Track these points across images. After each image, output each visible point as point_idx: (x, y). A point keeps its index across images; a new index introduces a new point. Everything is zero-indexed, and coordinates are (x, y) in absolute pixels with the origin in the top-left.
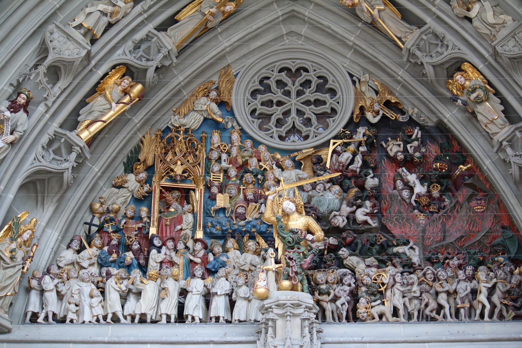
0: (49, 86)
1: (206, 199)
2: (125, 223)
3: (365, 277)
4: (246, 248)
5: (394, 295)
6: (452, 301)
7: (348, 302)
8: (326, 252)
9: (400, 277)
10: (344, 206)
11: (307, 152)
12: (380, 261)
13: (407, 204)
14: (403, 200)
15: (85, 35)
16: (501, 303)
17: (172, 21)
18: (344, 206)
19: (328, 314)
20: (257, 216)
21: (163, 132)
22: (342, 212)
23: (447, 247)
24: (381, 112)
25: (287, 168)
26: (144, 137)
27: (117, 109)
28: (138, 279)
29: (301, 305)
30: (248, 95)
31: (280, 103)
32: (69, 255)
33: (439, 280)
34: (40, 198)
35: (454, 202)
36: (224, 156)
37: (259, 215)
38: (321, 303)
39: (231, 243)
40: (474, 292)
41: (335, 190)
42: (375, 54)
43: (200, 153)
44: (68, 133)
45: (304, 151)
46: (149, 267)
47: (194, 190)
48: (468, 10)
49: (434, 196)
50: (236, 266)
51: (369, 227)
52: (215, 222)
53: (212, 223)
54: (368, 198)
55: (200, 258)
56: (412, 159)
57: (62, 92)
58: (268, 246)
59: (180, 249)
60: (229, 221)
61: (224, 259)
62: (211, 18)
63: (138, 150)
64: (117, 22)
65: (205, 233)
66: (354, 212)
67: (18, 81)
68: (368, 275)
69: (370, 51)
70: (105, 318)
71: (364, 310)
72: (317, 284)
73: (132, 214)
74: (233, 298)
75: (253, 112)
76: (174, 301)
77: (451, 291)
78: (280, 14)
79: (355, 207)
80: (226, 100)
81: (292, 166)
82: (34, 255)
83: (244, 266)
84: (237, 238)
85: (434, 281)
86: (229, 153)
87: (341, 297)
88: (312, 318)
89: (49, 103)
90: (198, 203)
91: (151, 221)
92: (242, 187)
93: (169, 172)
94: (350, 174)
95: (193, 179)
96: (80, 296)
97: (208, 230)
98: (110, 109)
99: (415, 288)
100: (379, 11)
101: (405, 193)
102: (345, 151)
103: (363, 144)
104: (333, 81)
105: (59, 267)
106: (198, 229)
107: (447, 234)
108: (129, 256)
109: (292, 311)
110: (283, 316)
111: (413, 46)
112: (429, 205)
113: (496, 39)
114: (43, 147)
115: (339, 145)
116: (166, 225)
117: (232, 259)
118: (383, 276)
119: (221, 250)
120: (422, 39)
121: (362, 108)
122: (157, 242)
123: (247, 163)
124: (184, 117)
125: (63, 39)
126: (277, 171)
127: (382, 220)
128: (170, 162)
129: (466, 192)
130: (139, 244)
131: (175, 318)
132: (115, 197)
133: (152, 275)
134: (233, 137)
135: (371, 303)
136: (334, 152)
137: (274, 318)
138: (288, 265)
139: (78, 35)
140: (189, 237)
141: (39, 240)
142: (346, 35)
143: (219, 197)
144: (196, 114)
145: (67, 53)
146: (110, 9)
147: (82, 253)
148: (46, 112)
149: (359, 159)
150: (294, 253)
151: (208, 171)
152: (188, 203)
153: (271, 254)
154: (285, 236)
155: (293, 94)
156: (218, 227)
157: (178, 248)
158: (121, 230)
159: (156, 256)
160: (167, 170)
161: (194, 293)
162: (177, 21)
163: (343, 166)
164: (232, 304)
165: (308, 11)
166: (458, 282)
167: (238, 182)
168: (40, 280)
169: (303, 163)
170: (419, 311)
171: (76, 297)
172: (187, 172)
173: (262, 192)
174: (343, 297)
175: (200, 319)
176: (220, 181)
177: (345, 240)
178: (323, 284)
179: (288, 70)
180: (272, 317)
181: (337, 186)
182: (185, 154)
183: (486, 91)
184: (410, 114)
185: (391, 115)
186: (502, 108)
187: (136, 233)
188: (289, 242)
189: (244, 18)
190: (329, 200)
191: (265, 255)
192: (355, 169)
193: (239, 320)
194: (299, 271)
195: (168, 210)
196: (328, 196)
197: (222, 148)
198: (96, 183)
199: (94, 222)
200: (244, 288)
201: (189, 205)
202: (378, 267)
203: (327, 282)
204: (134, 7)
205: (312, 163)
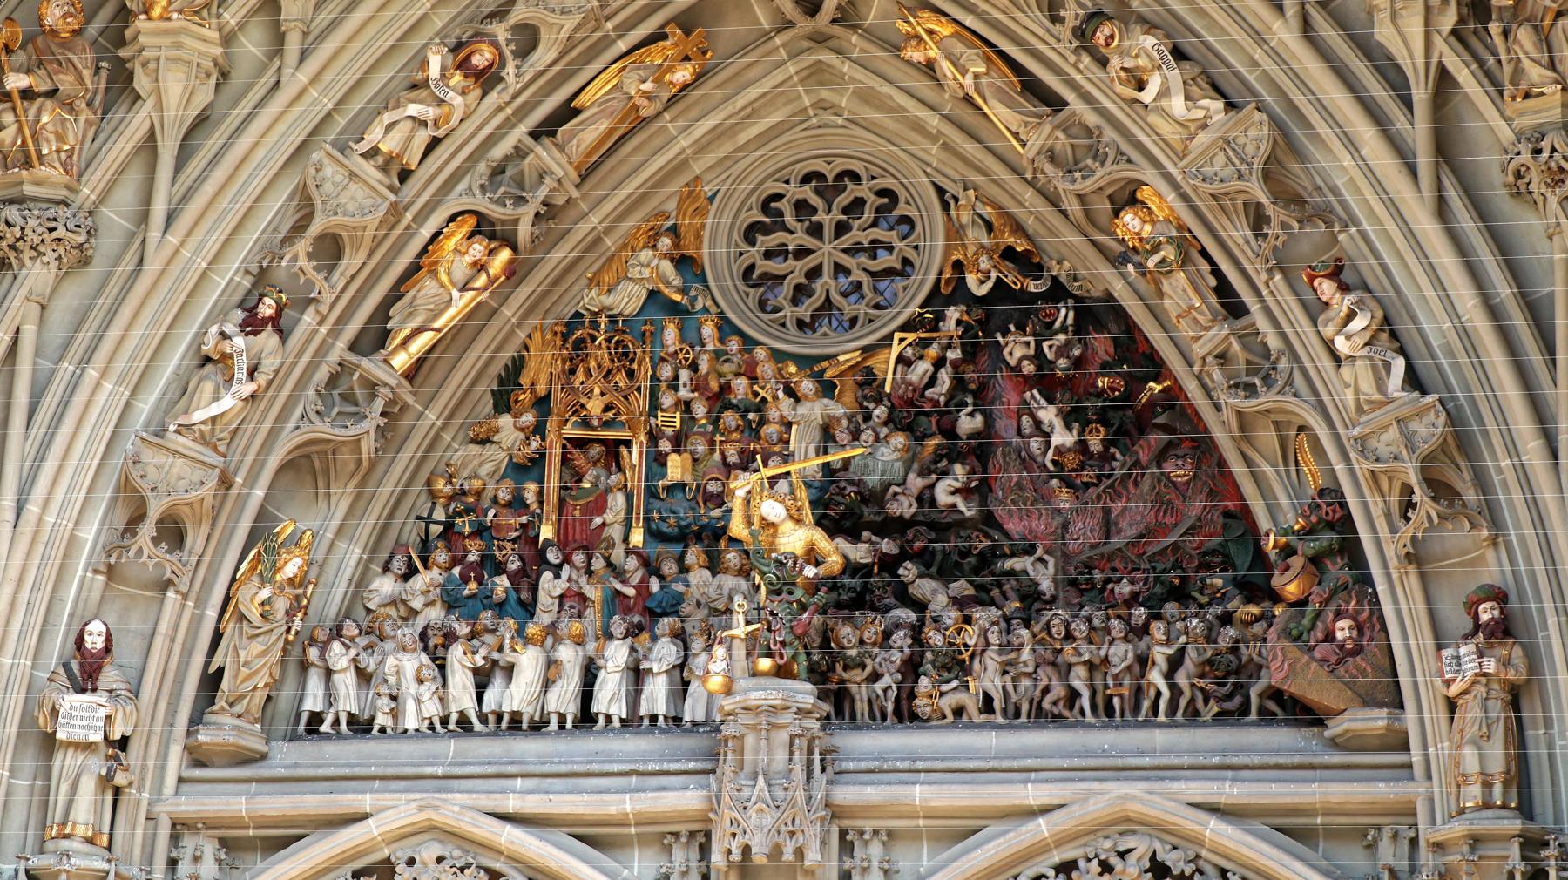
2: (495, 516)
8: (876, 568)
10: (911, 476)
11: (847, 361)
12: (979, 587)
15: (384, 169)
16: (1193, 685)
17: (567, 112)
19: (861, 707)
21: (568, 324)
24: (994, 275)
26: (530, 336)
29: (789, 708)
30: (735, 236)
31: (802, 253)
32: (385, 586)
36: (684, 375)
40: (1144, 661)
43: (639, 366)
44: (365, 363)
45: (841, 358)
46: (539, 606)
47: (628, 444)
48: (1141, 87)
49: (1092, 449)
50: (703, 601)
53: (659, 512)
57: (348, 283)
61: (680, 587)
63: (518, 365)
66: (932, 487)
67: (261, 267)
70: (445, 721)
73: (508, 497)
75: (751, 268)
76: (571, 687)
77: (1097, 661)
80: (690, 252)
82: (309, 602)
86: (694, 367)
89: (324, 309)
96: (399, 680)
97: (654, 526)
99: (1026, 655)
100: (976, 76)
101: (1035, 444)
102: (921, 357)
104: (908, 203)
105: (369, 611)
107: (1113, 528)
108: (503, 582)
110: (754, 728)
111: (1039, 153)
115: (910, 345)
119: (675, 568)
121: (958, 266)
122: (553, 556)
124: (609, 291)
126: (785, 403)
129: (1156, 438)
130: (521, 558)
131: (575, 717)
134: (703, 331)
136: (901, 359)
138: (769, 630)
139: (369, 170)
141: (321, 567)
146: (430, 113)
148: (320, 323)
149: (945, 376)
151: (655, 407)
155: (828, 232)
156: (672, 521)
163: (914, 390)
166: (1111, 643)
167: (710, 428)
168: (324, 647)
171: (392, 680)
175: (622, 720)
178: (851, 648)
179: (818, 176)
182: (609, 372)
184: (1054, 273)
185: (1012, 278)
186: (1213, 282)
187: (515, 534)
194: (789, 638)
197: (681, 356)
198: (437, 437)
203: (862, 642)
204: (483, 97)
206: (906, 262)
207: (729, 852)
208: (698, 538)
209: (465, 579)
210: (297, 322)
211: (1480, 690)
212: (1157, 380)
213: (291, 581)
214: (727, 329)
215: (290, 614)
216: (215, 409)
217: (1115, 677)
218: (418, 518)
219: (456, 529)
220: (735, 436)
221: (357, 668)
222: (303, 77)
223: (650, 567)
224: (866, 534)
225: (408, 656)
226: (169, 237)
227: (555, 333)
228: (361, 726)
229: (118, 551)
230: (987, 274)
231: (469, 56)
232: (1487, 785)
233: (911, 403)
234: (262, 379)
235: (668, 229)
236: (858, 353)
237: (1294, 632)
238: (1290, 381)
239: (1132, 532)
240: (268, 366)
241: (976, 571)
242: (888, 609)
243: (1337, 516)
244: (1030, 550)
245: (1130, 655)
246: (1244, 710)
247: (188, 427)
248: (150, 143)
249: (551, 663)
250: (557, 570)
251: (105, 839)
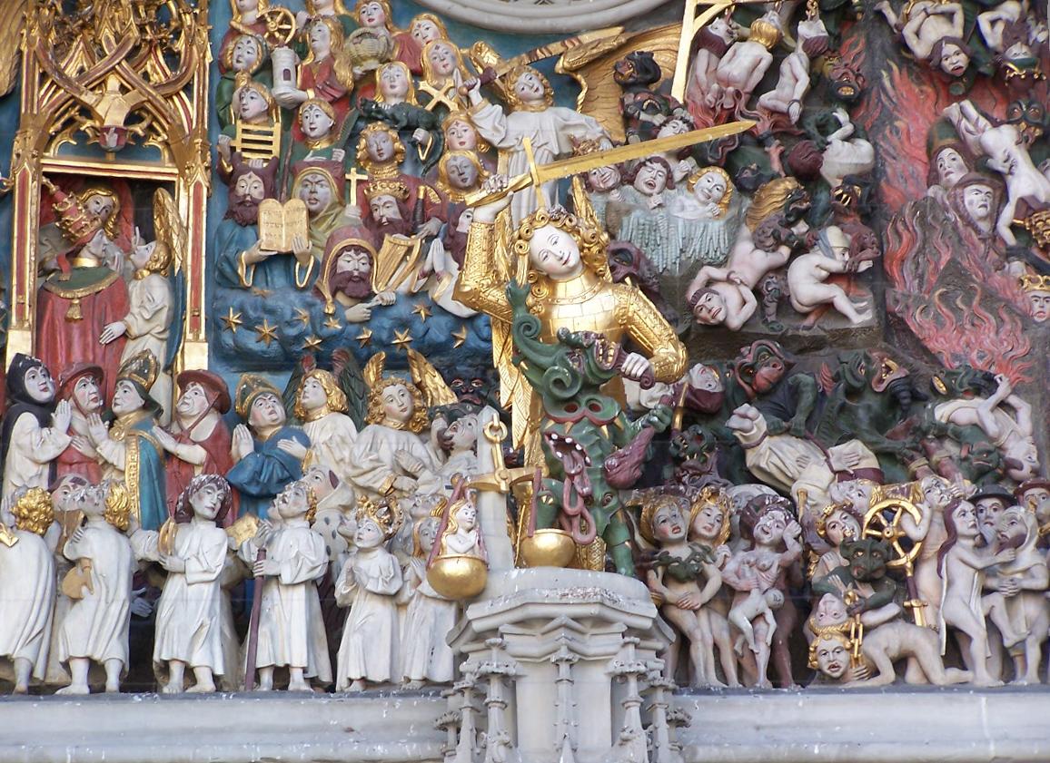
1: (217, 221)
3: (837, 516)
4: (377, 404)
5: (950, 584)
7: (777, 612)
8: (678, 419)
9: (970, 516)
11: (600, 41)
13: (984, 240)
14: (969, 223)
18: (745, 247)
19: (701, 655)
20: (410, 283)
22: (735, 268)
25: (524, 101)
36: (284, 58)
37: (423, 281)
38: (674, 613)
39: (319, 388)
41: (710, 186)
45: (586, 38)
50: (340, 475)
51: (841, 325)
52: (255, 309)
53: (241, 309)
54: (836, 215)
55: (202, 444)
56: (1000, 70)
58: (455, 400)
59: (123, 413)
60: (309, 306)
61: (293, 447)
65: (219, 352)
66: (782, 269)
68: (849, 510)
71: (838, 641)
72: (658, 544)
74: (337, 595)
79: (785, 251)
81: (544, 97)
83: (369, 476)
84: (339, 368)
86: (301, 48)
87: (748, 592)
88: (651, 670)
90: (186, 238)
91: (9, 306)
95: (166, 143)
97: (228, 339)
101: (976, 199)
102: (743, 39)
106: (189, 336)
110: (540, 661)
115: (720, 14)
116: (69, 320)
117: (324, 447)
118: (904, 511)
122: (36, 386)
123: (374, 85)
126: (488, 117)
127: (890, 302)
128: (80, 79)
133: (31, 511)
135: (862, 613)
136: (702, 40)
137: (512, 671)
138: (557, 473)
140: (157, 364)
143: (270, 212)
149: (796, 65)
150: (578, 426)
152: (148, 236)
153: (491, 427)
154: (543, 360)
156: (266, 329)
157: (116, 409)
159: (35, 438)
160: (66, 111)
161: (191, 578)
163: (738, 94)
164: (333, 617)
167: (340, 155)
169: (583, 82)
172: (141, 119)
173: (432, 194)
174: (755, 592)
175: (216, 678)
176: (270, 152)
177: (753, 376)
178: (678, 542)
180: (502, 670)
181: (718, 170)
182: (136, 49)
188: (559, 383)
190: (690, 223)
191: (448, 434)
192: (783, 107)
193: (363, 679)
195: (72, 263)
196: (683, 208)
197: (272, 25)
201: (153, 244)
202: (879, 477)
203: (692, 535)
205: (618, 82)
208: (324, 363)
241: (880, 424)
244: (983, 385)
249: (64, 566)
250: (45, 412)
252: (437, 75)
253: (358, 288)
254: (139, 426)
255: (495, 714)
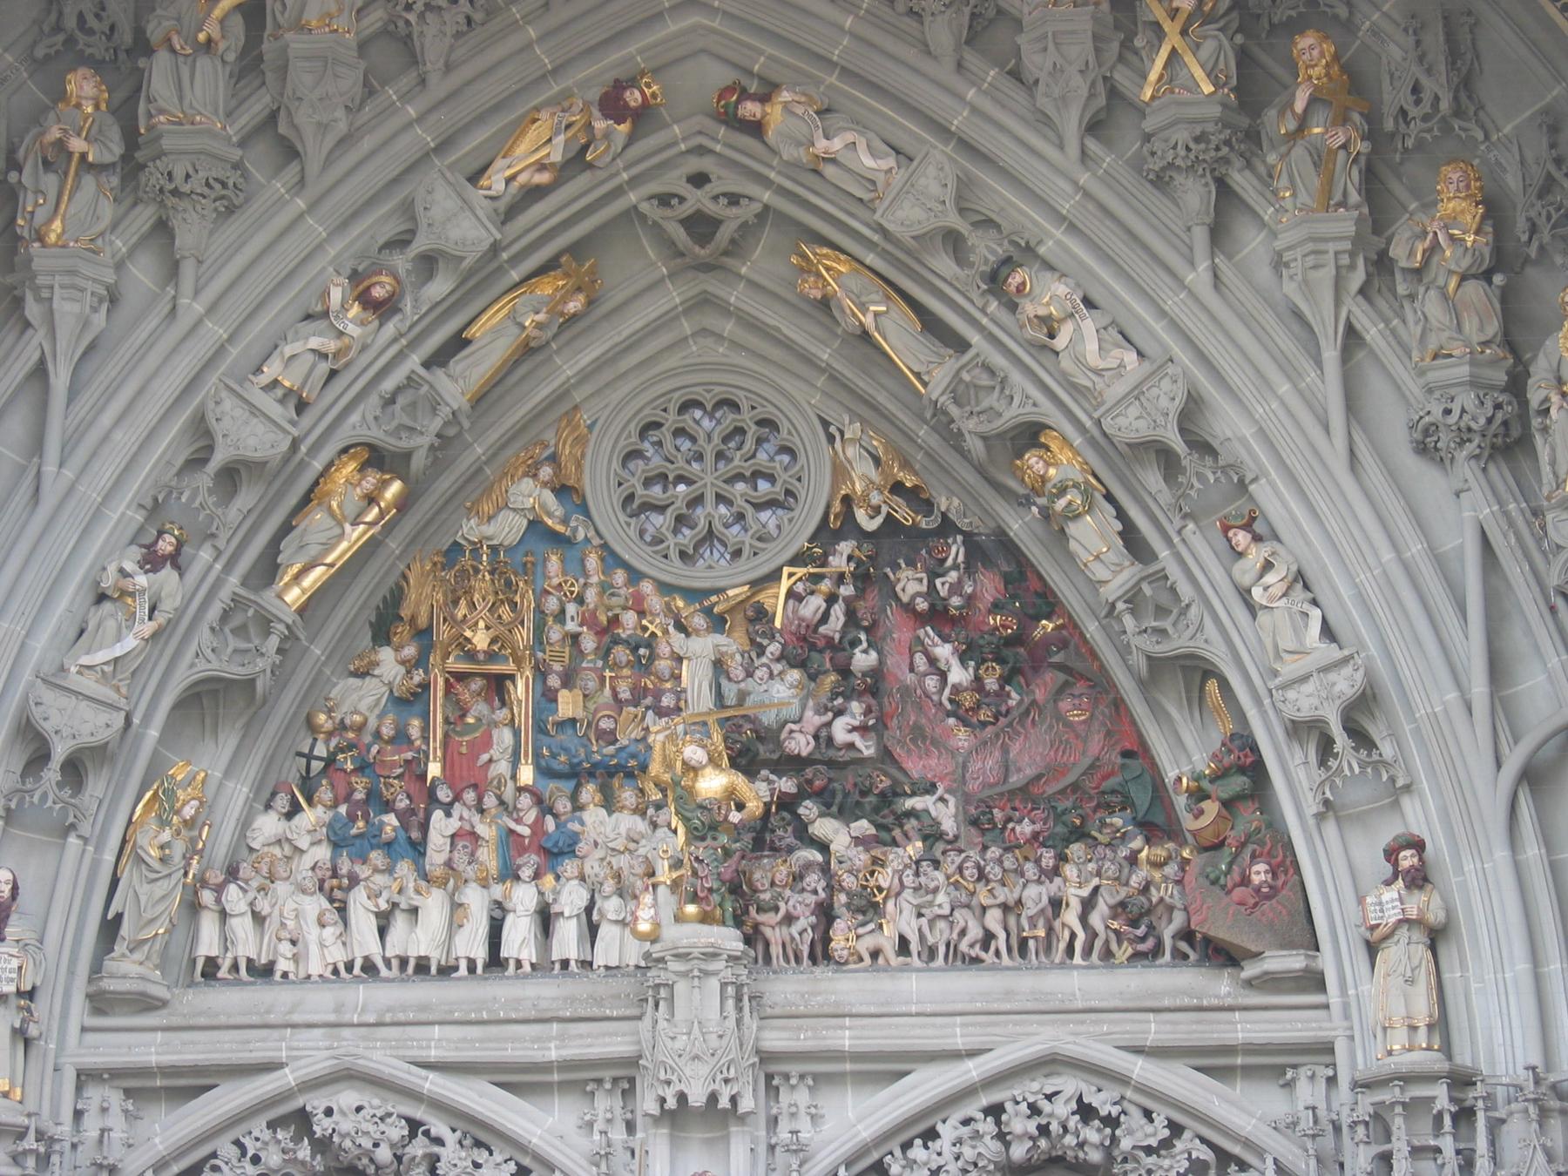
0: (219, 511)
1: (538, 695)
6: (1012, 921)
7: (813, 928)
10: (809, 713)
12: (878, 826)
14: (928, 696)
15: (282, 401)
16: (1107, 927)
19: (776, 950)
20: (637, 733)
23: (1012, 793)
24: (885, 509)
25: (697, 632)
27: (355, 535)
28: (411, 885)
30: (616, 465)
32: (268, 825)
33: (988, 881)
34: (208, 721)
35: (1027, 701)
39: (589, 792)
40: (1057, 904)
42: (871, 391)
43: (522, 597)
45: (731, 593)
46: (431, 847)
47: (512, 677)
48: (1052, 336)
53: (549, 748)
54: (859, 695)
56: (946, 610)
60: (585, 746)
61: (575, 826)
62: (536, 333)
63: (396, 596)
64: (347, 365)
66: (829, 724)
67: (156, 500)
69: (862, 383)
70: (349, 967)
71: (843, 943)
72: (755, 891)
73: (392, 733)
75: (630, 498)
77: (1011, 902)
78: (678, 300)
79: (830, 714)
80: (571, 482)
85: (979, 879)
86: (580, 600)
87: (798, 918)
89: (221, 544)
92: (608, 674)
93: (463, 643)
94: (821, 644)
97: (543, 763)
98: (342, 536)
100: (876, 314)
101: (931, 683)
102: (812, 593)
103: (848, 579)
105: (251, 850)
107: (1012, 768)
108: (391, 820)
109: (703, 966)
110: (685, 975)
111: (943, 393)
112: (978, 706)
113: (1102, 403)
114: (212, 629)
115: (800, 579)
119: (569, 805)
120: (961, 380)
121: (847, 500)
122: (444, 794)
125: (240, 412)
126: (677, 638)
129: (1052, 678)
130: (409, 797)
132: (355, 696)
136: (791, 594)
138: (695, 873)
139: (268, 404)
142: (813, 350)
143: (564, 695)
144: (512, 515)
145: (252, 442)
147: (297, 819)
148: (216, 559)
149: (838, 611)
152: (503, 703)
154: (689, 815)
155: (709, 457)
156: (563, 758)
158: (369, 765)
162: (468, 342)
165: (735, 296)
166: (1025, 886)
167: (600, 663)
168: (219, 889)
170: (948, 945)
171: (291, 924)
175: (532, 965)
179: (698, 404)
183: (1087, 494)
185: (905, 515)
186: (1119, 526)
187: (400, 771)
189: (607, 316)
198: (320, 672)
199: (316, 753)
200: (615, 902)
203: (773, 884)
206: (789, 493)
207: (663, 1100)
208: (591, 774)
209: (352, 818)
210: (194, 557)
211: (1403, 933)
212: (1048, 618)
213: (189, 824)
214: (610, 561)
215: (187, 859)
216: (118, 651)
217: (1030, 918)
218: (300, 754)
219: (338, 765)
220: (626, 672)
221: (253, 912)
222: (199, 308)
223: (544, 806)
224: (764, 772)
225: (307, 899)
226: (64, 471)
227: (435, 564)
228: (263, 971)
229: (19, 795)
230: (877, 510)
231: (368, 289)
232: (1413, 1029)
233: (804, 639)
234: (161, 618)
235: (547, 459)
236: (746, 588)
237: (1212, 876)
238: (1200, 627)
239: (1030, 772)
240: (168, 606)
242: (791, 850)
243: (1249, 760)
244: (930, 789)
245: (1045, 900)
246: (1157, 951)
247: (89, 667)
248: (40, 372)
249: (456, 907)
251: (18, 1091)
252: (652, 614)
253: (610, 737)
254: (495, 816)
255: (662, 1003)
